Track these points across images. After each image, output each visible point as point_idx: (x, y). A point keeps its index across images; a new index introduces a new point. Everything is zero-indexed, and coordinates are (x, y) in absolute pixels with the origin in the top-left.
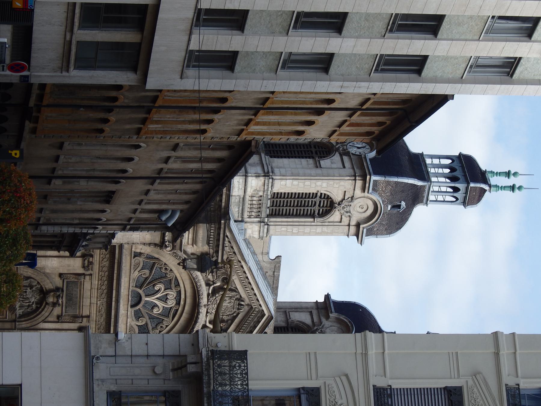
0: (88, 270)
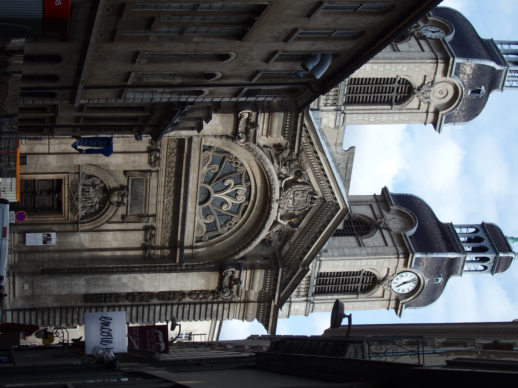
0: (155, 166)
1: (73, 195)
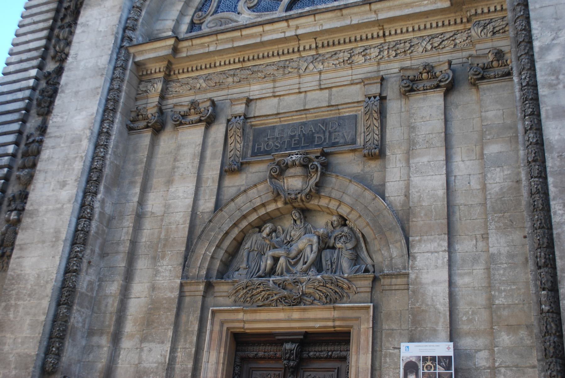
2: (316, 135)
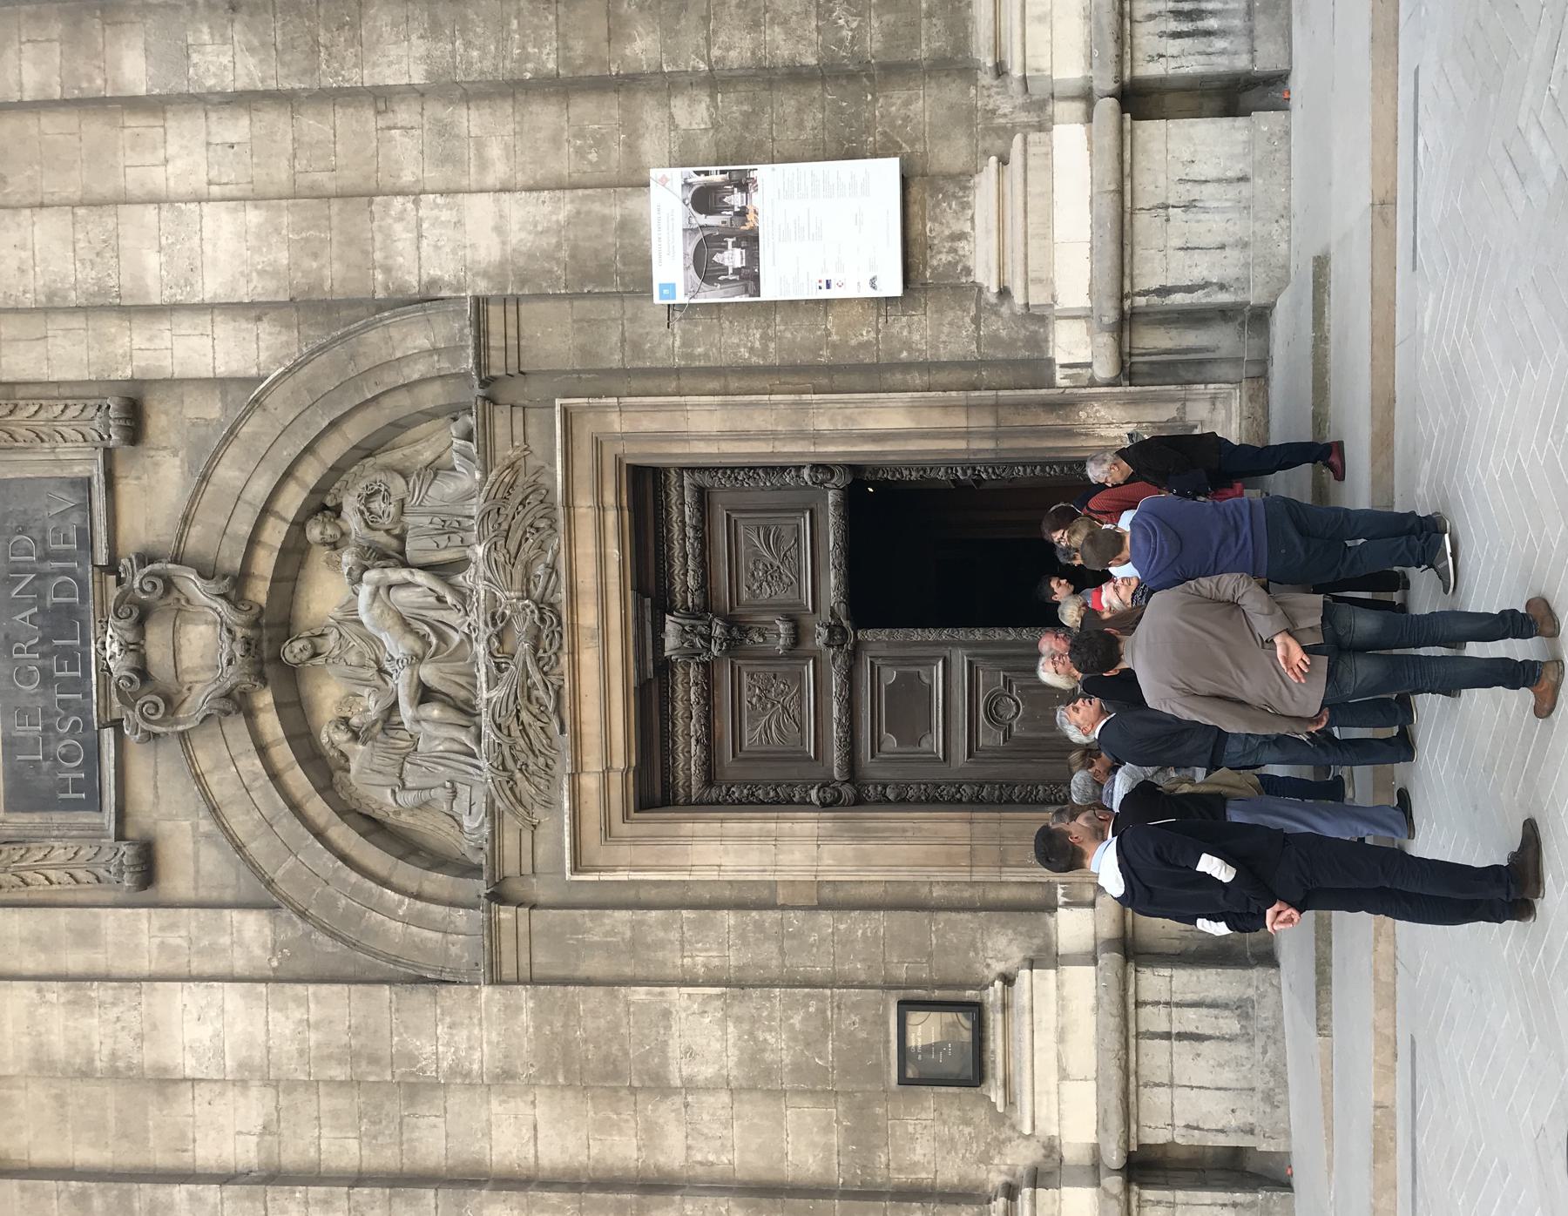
1: (536, 677)
2: (51, 599)
